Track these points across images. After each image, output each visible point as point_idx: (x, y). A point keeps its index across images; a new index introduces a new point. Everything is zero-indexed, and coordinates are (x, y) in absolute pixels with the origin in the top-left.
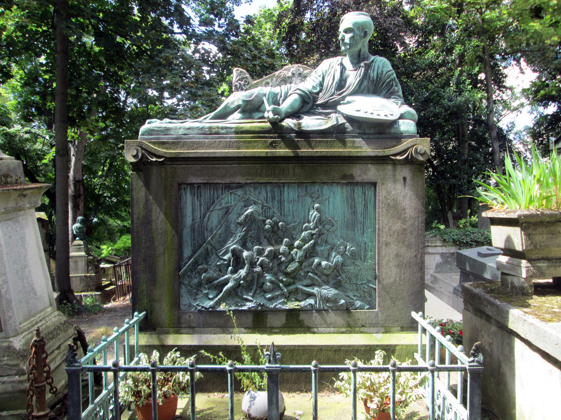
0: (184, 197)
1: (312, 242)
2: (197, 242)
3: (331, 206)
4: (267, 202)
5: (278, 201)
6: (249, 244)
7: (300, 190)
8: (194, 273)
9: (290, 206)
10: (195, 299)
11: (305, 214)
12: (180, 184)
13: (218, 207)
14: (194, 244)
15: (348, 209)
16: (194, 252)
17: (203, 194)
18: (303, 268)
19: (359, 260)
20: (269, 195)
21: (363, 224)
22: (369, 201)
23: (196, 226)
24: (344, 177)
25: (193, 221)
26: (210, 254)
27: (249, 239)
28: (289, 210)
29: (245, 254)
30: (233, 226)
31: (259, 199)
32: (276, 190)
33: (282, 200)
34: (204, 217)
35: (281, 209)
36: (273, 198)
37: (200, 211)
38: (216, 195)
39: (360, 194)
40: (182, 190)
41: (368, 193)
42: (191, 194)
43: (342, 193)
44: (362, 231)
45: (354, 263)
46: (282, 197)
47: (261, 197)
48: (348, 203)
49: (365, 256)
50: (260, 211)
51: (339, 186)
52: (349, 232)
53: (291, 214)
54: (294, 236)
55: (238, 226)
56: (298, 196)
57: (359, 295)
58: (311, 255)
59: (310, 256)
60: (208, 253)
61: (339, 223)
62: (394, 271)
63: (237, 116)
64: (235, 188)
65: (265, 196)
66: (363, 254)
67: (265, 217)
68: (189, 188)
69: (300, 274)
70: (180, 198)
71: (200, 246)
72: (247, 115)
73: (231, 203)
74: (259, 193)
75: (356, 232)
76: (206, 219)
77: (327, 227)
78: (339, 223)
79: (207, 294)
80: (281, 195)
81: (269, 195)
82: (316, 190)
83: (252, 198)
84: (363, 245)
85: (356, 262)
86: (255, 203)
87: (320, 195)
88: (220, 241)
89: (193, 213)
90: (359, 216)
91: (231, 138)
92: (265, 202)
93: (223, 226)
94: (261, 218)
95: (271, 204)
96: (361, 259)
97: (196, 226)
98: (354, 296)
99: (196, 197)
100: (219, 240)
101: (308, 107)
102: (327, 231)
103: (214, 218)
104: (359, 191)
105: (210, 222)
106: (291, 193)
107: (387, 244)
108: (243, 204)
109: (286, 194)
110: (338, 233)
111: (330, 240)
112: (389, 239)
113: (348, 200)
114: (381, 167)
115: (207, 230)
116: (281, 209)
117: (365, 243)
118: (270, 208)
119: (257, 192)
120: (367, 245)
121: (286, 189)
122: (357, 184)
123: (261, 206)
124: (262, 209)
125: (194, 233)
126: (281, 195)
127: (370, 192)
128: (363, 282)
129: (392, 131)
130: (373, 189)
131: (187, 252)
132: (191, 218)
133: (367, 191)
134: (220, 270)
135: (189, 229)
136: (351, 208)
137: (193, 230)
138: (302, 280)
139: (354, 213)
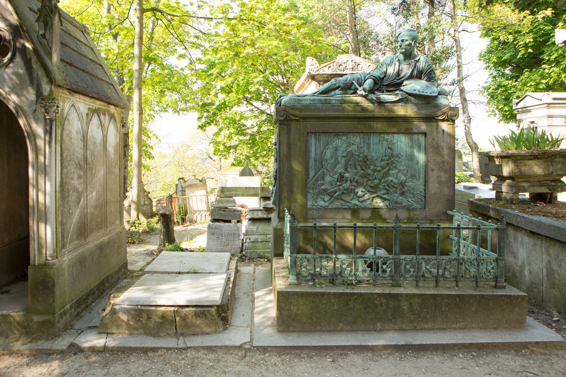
1: (387, 168)
6: (349, 169)
10: (316, 202)
12: (308, 133)
20: (362, 140)
24: (407, 129)
27: (349, 166)
29: (347, 175)
30: (339, 158)
31: (355, 142)
32: (366, 137)
34: (322, 153)
36: (364, 142)
49: (419, 177)
50: (356, 149)
51: (404, 135)
60: (324, 175)
62: (437, 185)
63: (337, 92)
68: (313, 136)
70: (307, 141)
71: (320, 170)
72: (344, 92)
76: (323, 154)
77: (396, 159)
79: (324, 198)
83: (351, 141)
86: (353, 144)
91: (338, 106)
94: (357, 153)
101: (378, 86)
103: (328, 154)
104: (416, 137)
106: (375, 139)
107: (433, 170)
108: (346, 145)
109: (372, 139)
110: (403, 163)
111: (398, 167)
112: (433, 167)
114: (429, 124)
119: (354, 138)
121: (372, 136)
122: (415, 133)
129: (435, 102)
130: (424, 137)
131: (312, 174)
134: (332, 185)
135: (313, 160)
137: (315, 160)
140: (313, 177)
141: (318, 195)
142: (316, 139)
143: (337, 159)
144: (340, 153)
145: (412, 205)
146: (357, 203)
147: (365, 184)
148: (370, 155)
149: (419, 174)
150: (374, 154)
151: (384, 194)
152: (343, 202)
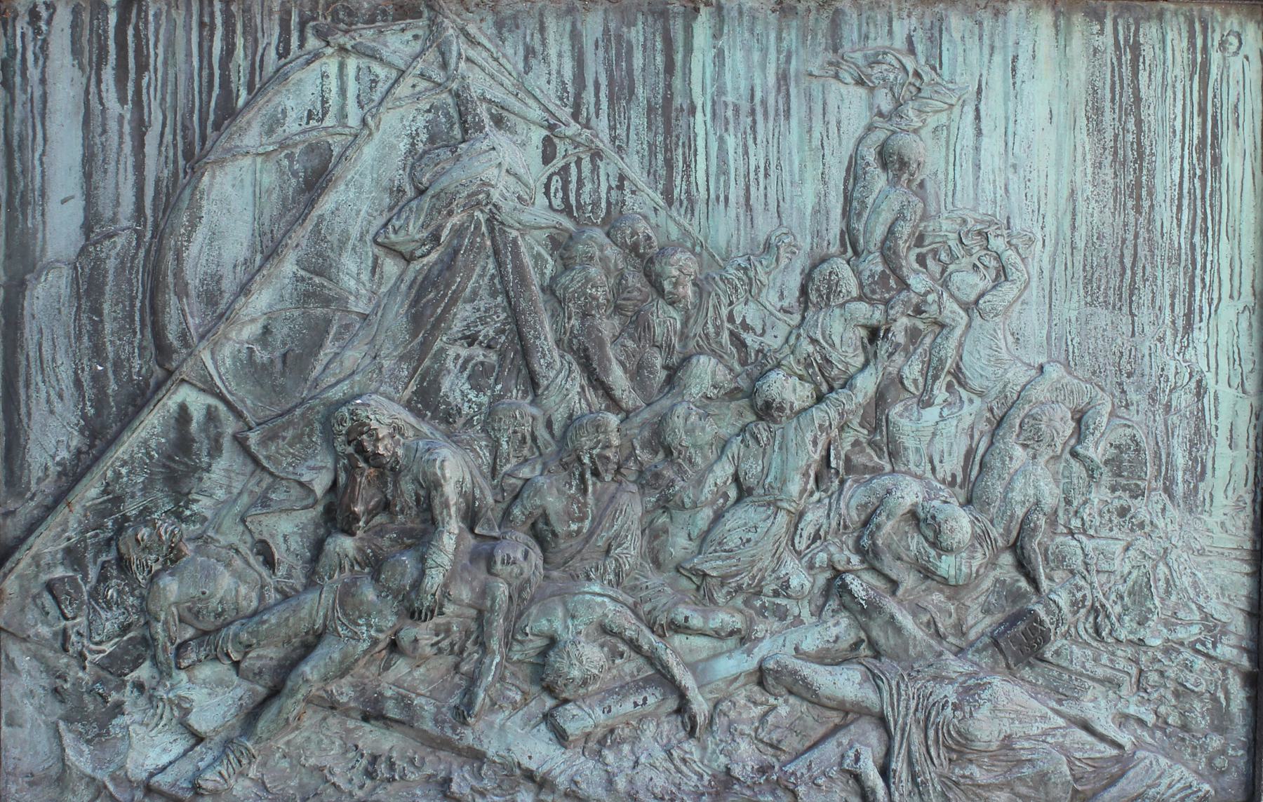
0: (34, 73)
2: (118, 365)
3: (992, 145)
4: (575, 116)
5: (650, 110)
7: (791, 37)
8: (93, 574)
9: (731, 142)
11: (822, 197)
13: (252, 137)
14: (97, 378)
15: (1098, 165)
16: (98, 437)
17: (156, 55)
18: (801, 544)
19: (1159, 497)
20: (595, 67)
21: (1193, 267)
22: (1227, 116)
23: (111, 264)
25: (87, 228)
26: (202, 446)
28: (723, 170)
30: (351, 273)
31: (522, 89)
32: (636, 34)
33: (678, 101)
35: (669, 164)
36: (621, 92)
37: (139, 167)
38: (239, 52)
39: (1178, 71)
40: (22, 25)
41: (1225, 67)
42: (76, 52)
43: (1064, 62)
44: (1180, 309)
45: (1123, 512)
46: (678, 83)
47: (539, 80)
48: (1097, 129)
50: (535, 171)
52: (1103, 317)
53: (735, 193)
54: (749, 338)
55: (391, 267)
56: (783, 78)
57: (1151, 719)
58: (859, 459)
59: (850, 466)
61: (1040, 256)
64: (372, 20)
65: (568, 73)
66: (1181, 459)
67: (567, 210)
69: (786, 585)
71: (140, 399)
73: (342, 115)
74: (529, 52)
75: (1144, 316)
78: (1040, 256)
80: (669, 68)
81: (595, 67)
82: (899, 42)
84: (1183, 400)
85: (1142, 510)
87: (926, 72)
88: (265, 368)
89: (88, 176)
90: (1165, 214)
92: (565, 113)
93: (289, 266)
95: (602, 124)
96: (1167, 490)
97: (111, 264)
98: (1124, 719)
99: (108, 74)
100: (261, 355)
102: (966, 307)
105: (200, 235)
106: (736, 60)
111: (976, 366)
113: (1098, 111)
115: (182, 292)
116: (669, 164)
117: (1200, 391)
118: (596, 155)
119: (512, 51)
120: (1207, 401)
123: (538, 135)
124: (547, 158)
125: (97, 310)
126: (669, 68)
127: (1236, 64)
128: (1181, 634)
132: (77, 206)
133: (1216, 57)
136: (1119, 163)
137: (88, 287)
138: (798, 621)
139: (1136, 194)
140: (73, 474)
141: (116, 666)
142: (90, 56)
143: (319, 266)
144: (352, 202)
145: (1124, 762)
146: (537, 750)
147: (631, 551)
148: (697, 248)
149: (1200, 436)
150: (723, 229)
151: (824, 658)
152: (387, 741)
